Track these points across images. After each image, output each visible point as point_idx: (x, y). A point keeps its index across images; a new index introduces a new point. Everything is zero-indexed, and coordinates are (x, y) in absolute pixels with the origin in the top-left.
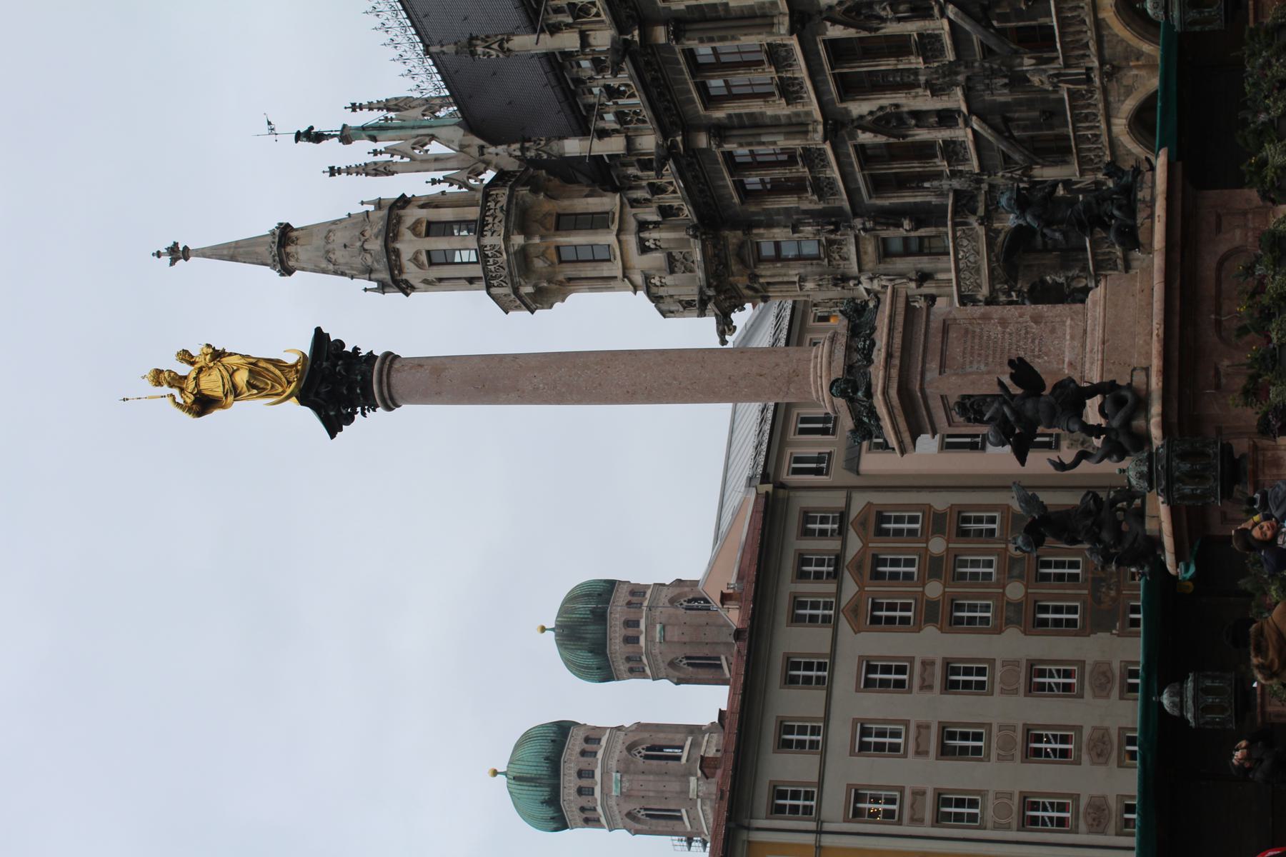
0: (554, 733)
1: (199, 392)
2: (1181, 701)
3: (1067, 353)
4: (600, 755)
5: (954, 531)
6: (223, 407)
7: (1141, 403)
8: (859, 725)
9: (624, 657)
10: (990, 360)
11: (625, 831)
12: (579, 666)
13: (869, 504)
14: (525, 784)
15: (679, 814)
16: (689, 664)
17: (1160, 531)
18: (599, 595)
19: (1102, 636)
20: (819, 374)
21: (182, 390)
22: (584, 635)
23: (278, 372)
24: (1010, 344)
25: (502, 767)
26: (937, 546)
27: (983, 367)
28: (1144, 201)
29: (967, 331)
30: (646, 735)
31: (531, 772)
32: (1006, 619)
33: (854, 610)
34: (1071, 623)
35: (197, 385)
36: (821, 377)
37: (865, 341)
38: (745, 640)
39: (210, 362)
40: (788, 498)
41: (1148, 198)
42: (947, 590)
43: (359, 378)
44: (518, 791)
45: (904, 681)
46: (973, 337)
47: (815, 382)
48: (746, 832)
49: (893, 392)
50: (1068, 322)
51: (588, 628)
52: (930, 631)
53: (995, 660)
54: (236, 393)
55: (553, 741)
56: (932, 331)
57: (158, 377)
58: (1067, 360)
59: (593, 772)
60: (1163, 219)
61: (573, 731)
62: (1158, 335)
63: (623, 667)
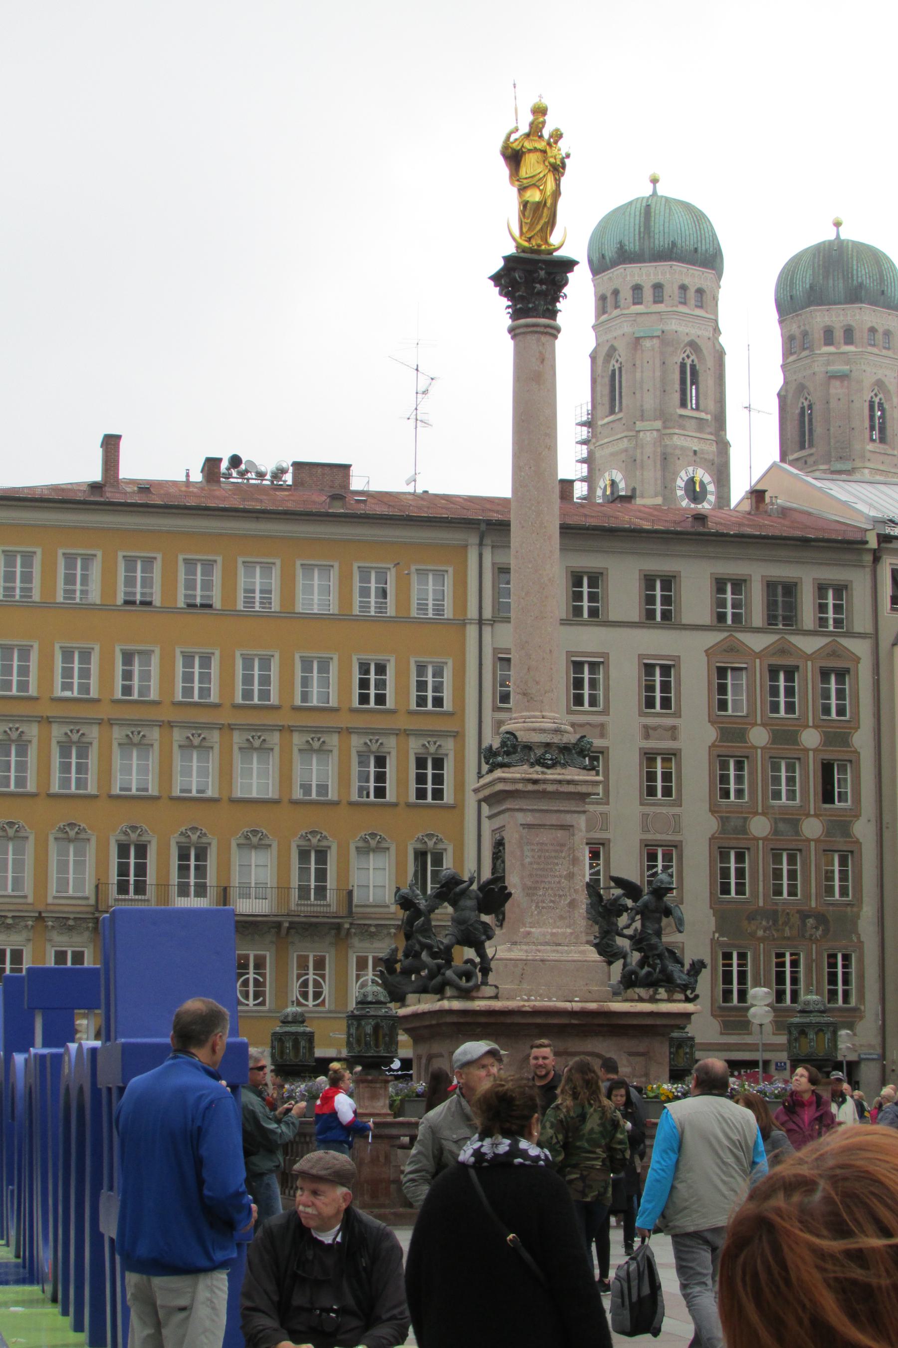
0: (706, 250)
1: (524, 153)
2: (289, 1022)
3: (539, 930)
4: (682, 309)
5: (828, 756)
6: (511, 176)
7: (465, 994)
8: (601, 660)
9: (807, 328)
10: (535, 866)
11: (594, 345)
12: (793, 272)
13: (857, 660)
14: (642, 219)
15: (617, 410)
16: (803, 409)
17: (408, 1006)
18: (883, 292)
19: (711, 923)
20: (527, 720)
21: (528, 135)
22: (831, 277)
23: (539, 227)
24: (550, 882)
25: (663, 190)
26: (811, 738)
27: (528, 860)
28: (656, 993)
29: (563, 845)
30: (710, 362)
31: (657, 225)
32: (727, 818)
33: (732, 649)
34: (725, 890)
35: (530, 151)
36: (524, 722)
37: (551, 759)
38: (693, 527)
39: (549, 163)
40: (864, 567)
41: (658, 997)
42: (759, 751)
43: (530, 306)
44: (632, 212)
45: (654, 707)
46: (556, 851)
47: (522, 717)
48: (478, 542)
49: (500, 787)
50: (569, 931)
51: (841, 281)
52: (711, 734)
53: (681, 806)
54: (522, 190)
55: (696, 250)
56: (562, 815)
57: (540, 111)
58: (533, 930)
59: (661, 302)
60: (632, 1010)
61: (709, 274)
62: (524, 1006)
63: (795, 329)
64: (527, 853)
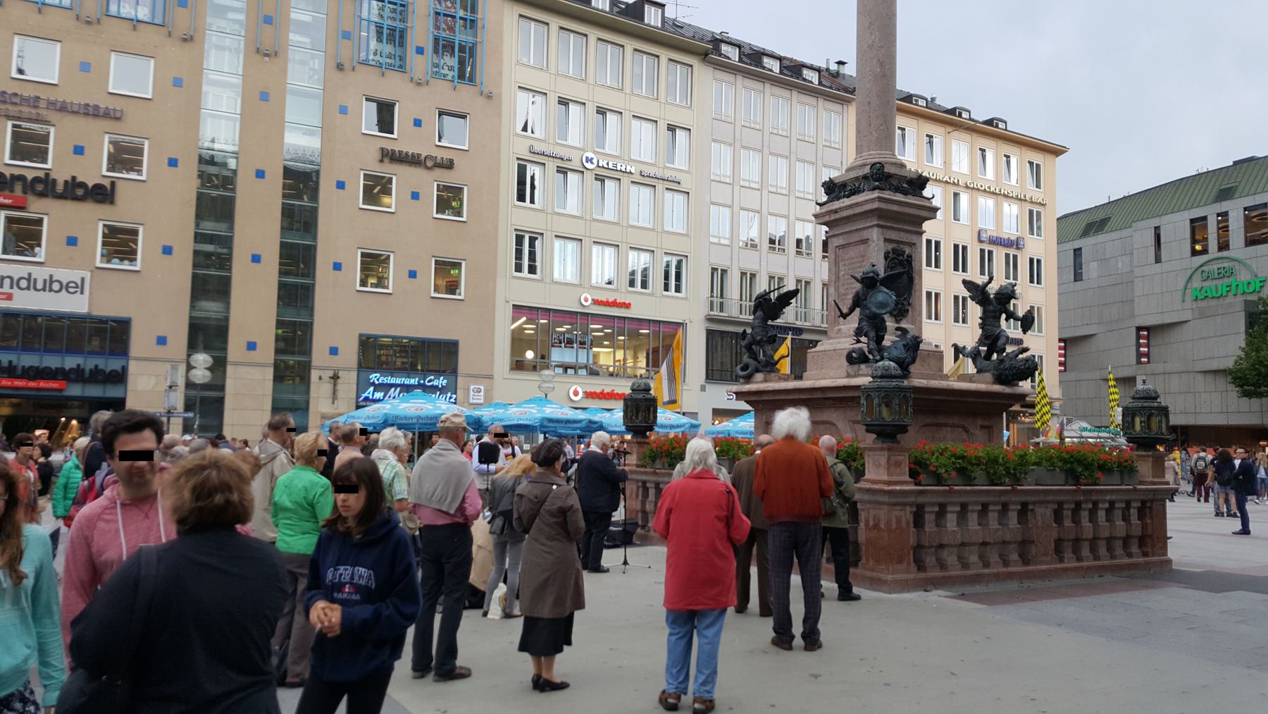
27: (842, 273)
28: (858, 370)
41: (861, 372)
58: (842, 327)
64: (841, 268)
